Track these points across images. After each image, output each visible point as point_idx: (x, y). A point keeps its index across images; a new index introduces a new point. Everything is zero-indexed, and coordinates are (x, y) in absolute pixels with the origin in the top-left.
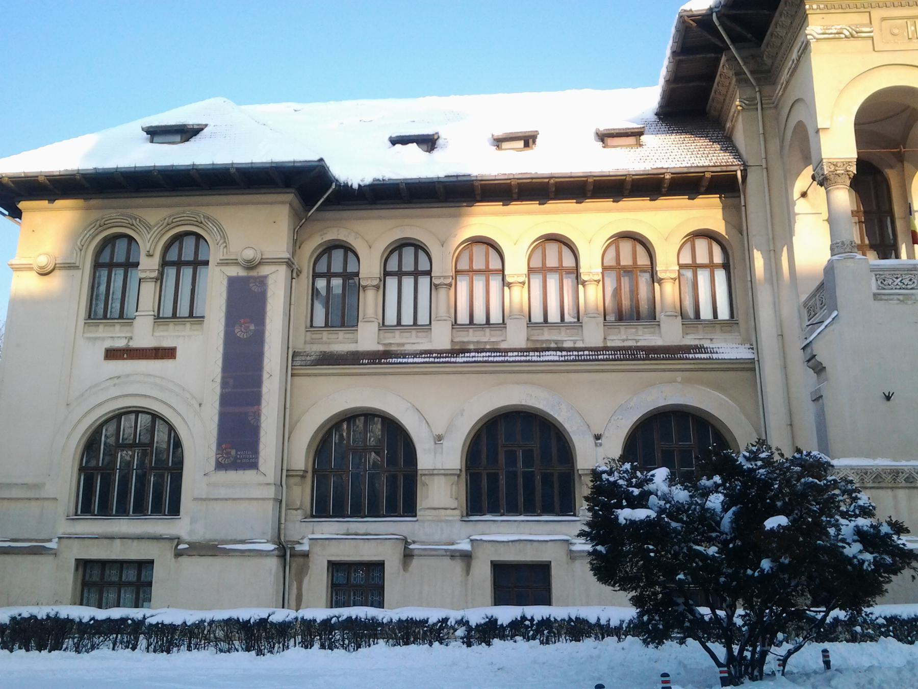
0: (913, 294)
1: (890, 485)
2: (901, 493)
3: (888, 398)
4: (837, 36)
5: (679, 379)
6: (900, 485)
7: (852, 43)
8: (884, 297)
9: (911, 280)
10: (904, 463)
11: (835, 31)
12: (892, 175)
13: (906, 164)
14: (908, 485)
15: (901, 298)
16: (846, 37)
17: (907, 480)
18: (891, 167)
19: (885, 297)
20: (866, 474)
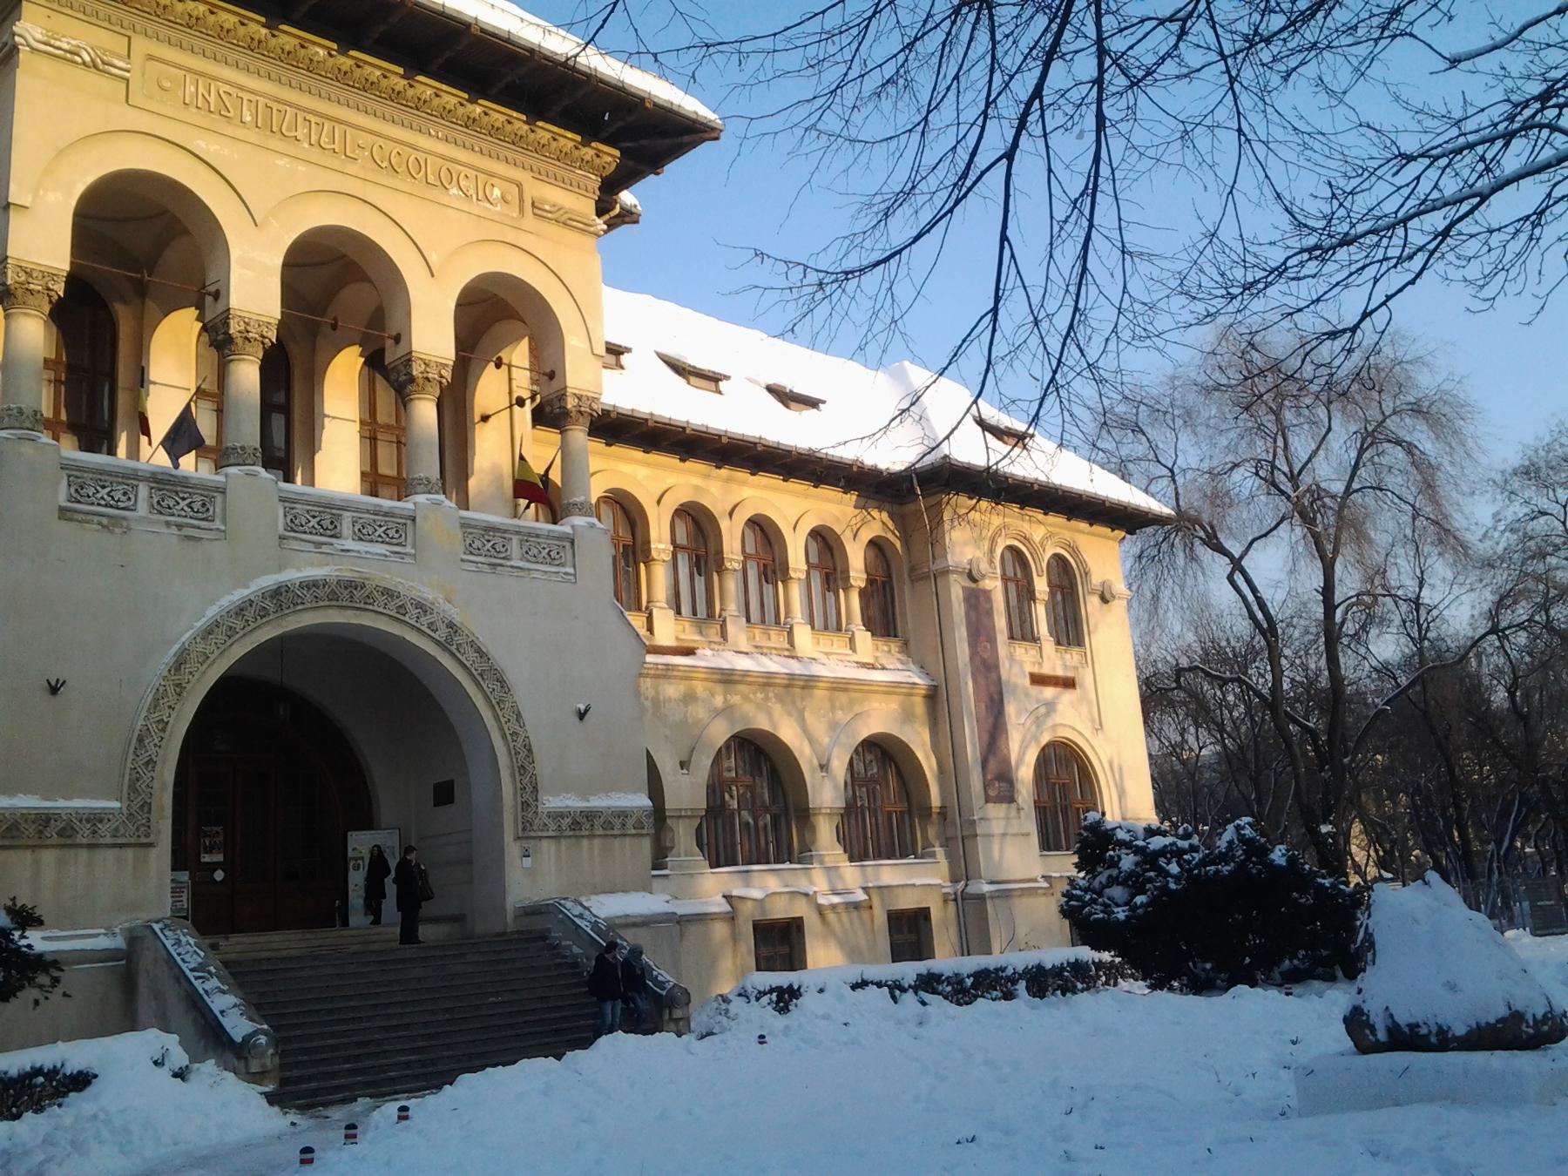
0: (124, 518)
1: (30, 842)
2: (48, 857)
3: (54, 690)
6: (49, 842)
8: (77, 516)
9: (125, 494)
10: (62, 803)
12: (124, 315)
13: (150, 304)
14: (62, 841)
15: (105, 521)
17: (61, 833)
18: (124, 301)
19: (80, 517)
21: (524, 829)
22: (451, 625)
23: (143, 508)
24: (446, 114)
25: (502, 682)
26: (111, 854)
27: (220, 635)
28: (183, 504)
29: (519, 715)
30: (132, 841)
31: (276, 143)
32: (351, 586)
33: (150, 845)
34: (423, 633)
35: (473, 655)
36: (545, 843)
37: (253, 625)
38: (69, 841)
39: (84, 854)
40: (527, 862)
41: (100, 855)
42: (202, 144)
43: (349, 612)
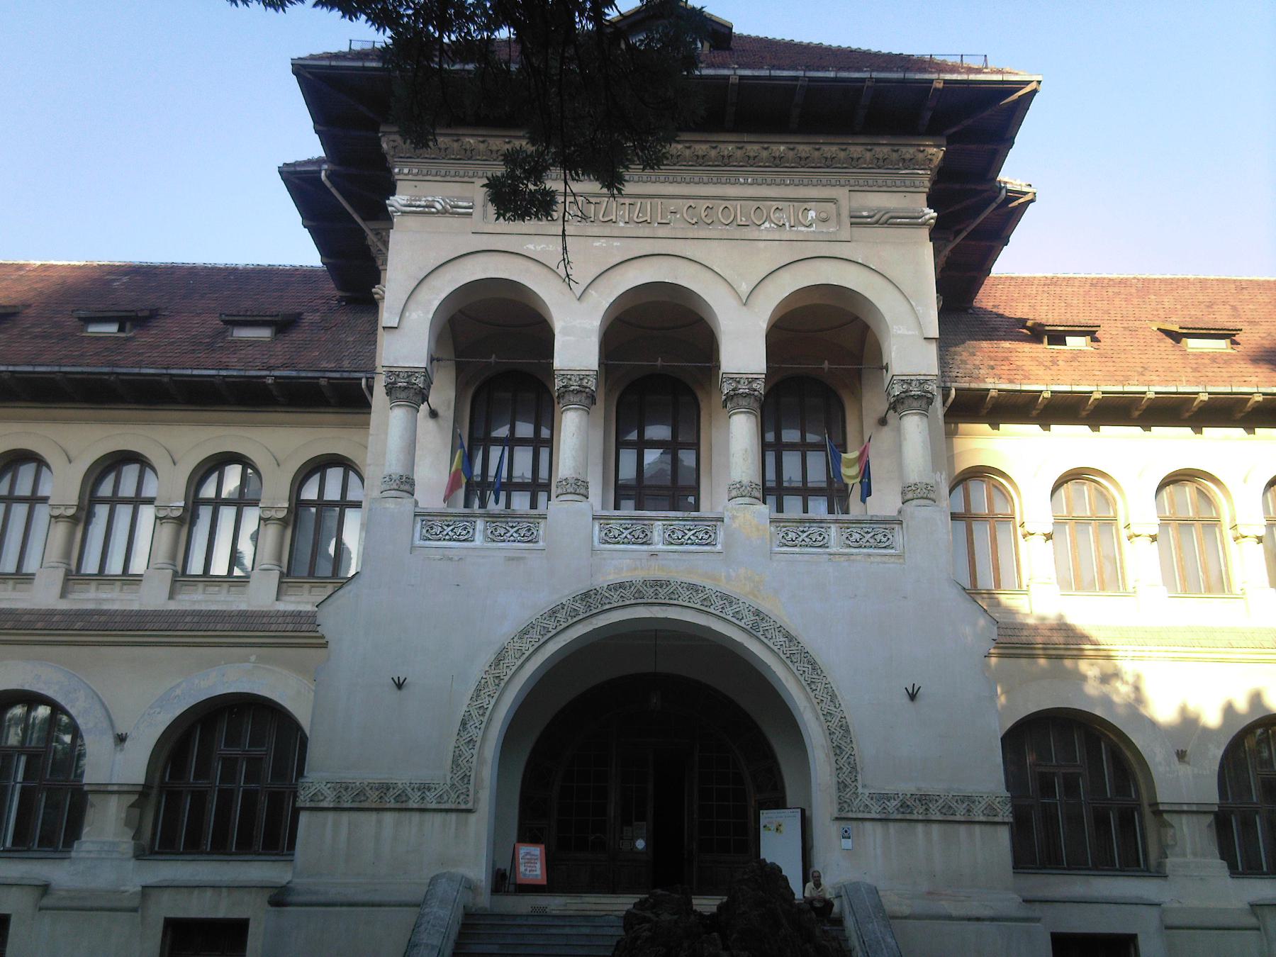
1: (374, 806)
2: (389, 818)
4: (427, 211)
5: (253, 658)
6: (388, 806)
11: (423, 203)
16: (438, 212)
17: (397, 798)
20: (346, 789)
21: (841, 810)
22: (757, 613)
23: (479, 539)
24: (751, 161)
25: (813, 664)
26: (439, 818)
27: (534, 635)
28: (512, 531)
29: (833, 697)
30: (453, 806)
31: (595, 230)
32: (658, 584)
33: (469, 811)
36: (868, 825)
37: (565, 625)
38: (404, 806)
39: (416, 817)
40: (847, 844)
41: (428, 816)
42: (531, 247)
43: (656, 608)
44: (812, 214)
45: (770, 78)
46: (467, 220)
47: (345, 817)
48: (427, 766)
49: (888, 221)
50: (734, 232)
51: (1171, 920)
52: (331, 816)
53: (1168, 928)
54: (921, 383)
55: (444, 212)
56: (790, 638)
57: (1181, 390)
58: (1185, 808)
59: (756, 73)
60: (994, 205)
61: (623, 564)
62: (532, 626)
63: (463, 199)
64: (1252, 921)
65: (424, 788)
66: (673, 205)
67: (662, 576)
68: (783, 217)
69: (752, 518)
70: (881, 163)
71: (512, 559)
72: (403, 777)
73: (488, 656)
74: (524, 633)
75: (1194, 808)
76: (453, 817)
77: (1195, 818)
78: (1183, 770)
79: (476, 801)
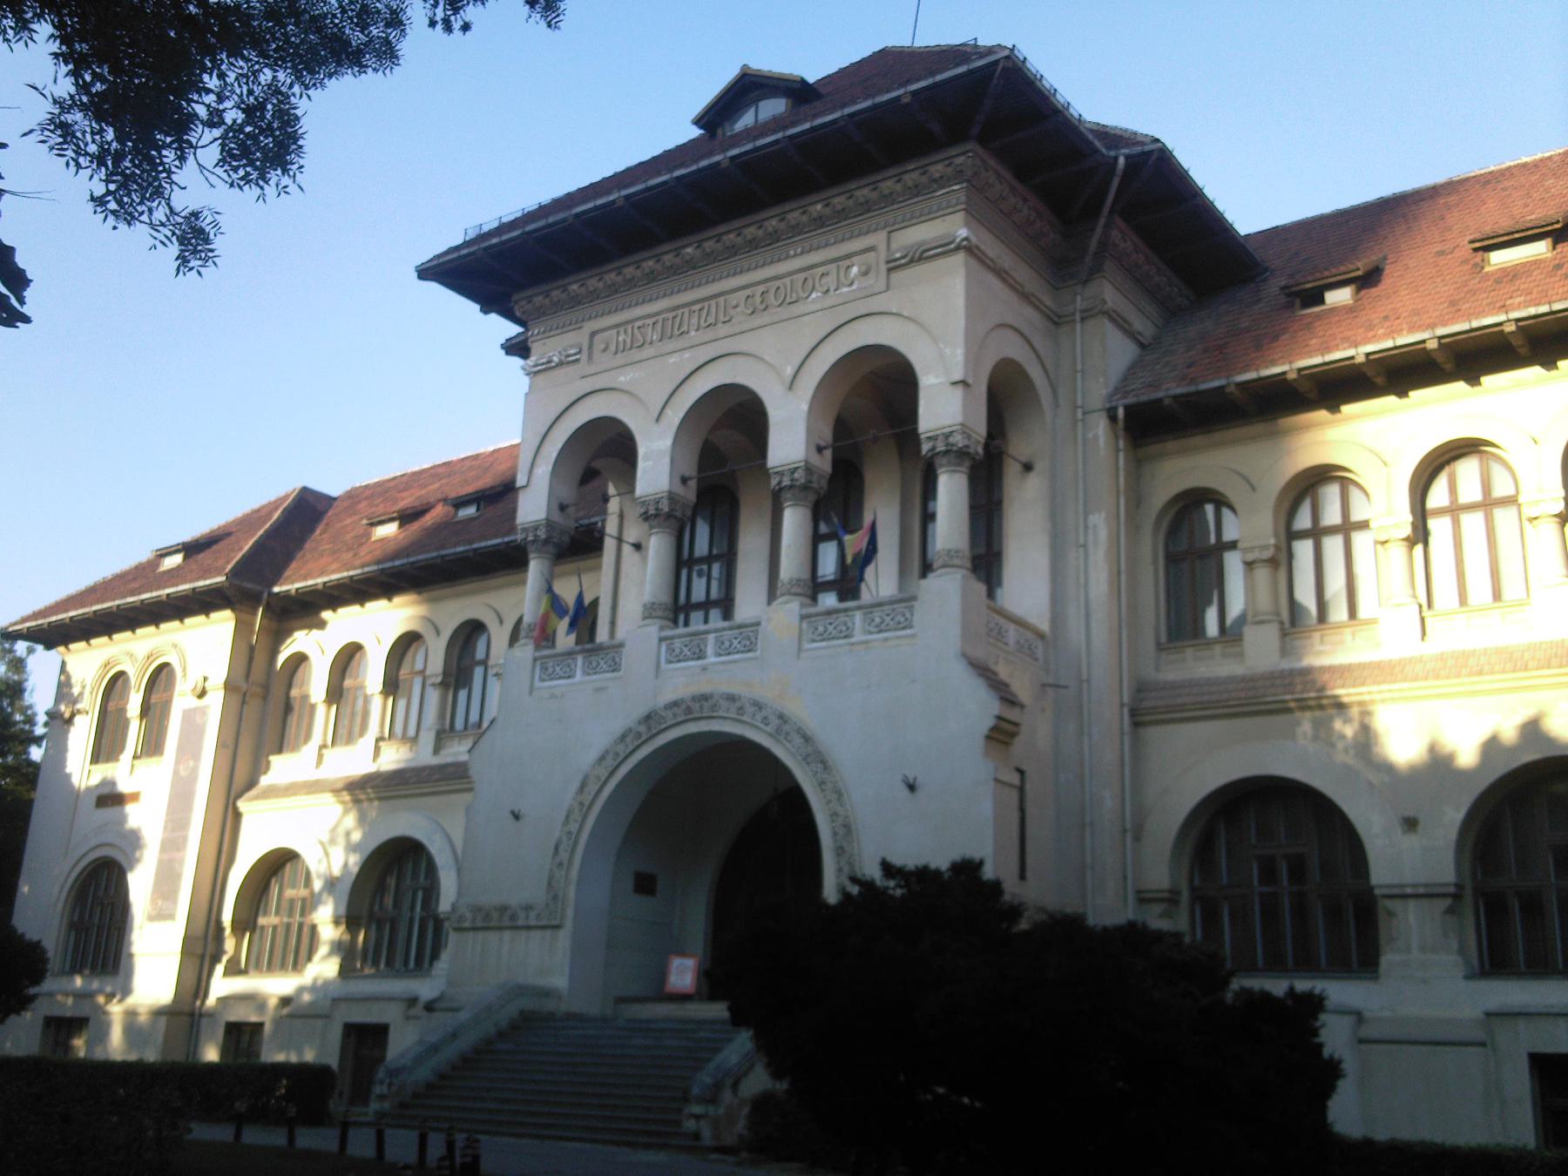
2: (507, 935)
7: (569, 370)
22: (781, 717)
23: (579, 673)
24: (797, 230)
32: (704, 698)
34: (757, 728)
35: (798, 740)
39: (524, 933)
42: (622, 379)
44: (855, 270)
45: (757, 149)
46: (576, 366)
47: (481, 935)
48: (526, 890)
49: (920, 256)
50: (786, 312)
51: (1365, 1032)
52: (471, 934)
53: (1361, 1041)
54: (947, 436)
55: (561, 364)
56: (807, 739)
57: (1401, 341)
58: (1409, 891)
59: (743, 149)
60: (1116, 182)
61: (681, 682)
62: (607, 752)
63: (572, 347)
64: (1479, 1035)
65: (528, 908)
66: (734, 299)
67: (705, 688)
68: (830, 281)
69: (785, 615)
70: (916, 191)
71: (598, 690)
72: (514, 900)
73: (576, 785)
74: (602, 758)
75: (1421, 890)
76: (548, 933)
77: (1425, 902)
78: (1411, 842)
79: (563, 917)
